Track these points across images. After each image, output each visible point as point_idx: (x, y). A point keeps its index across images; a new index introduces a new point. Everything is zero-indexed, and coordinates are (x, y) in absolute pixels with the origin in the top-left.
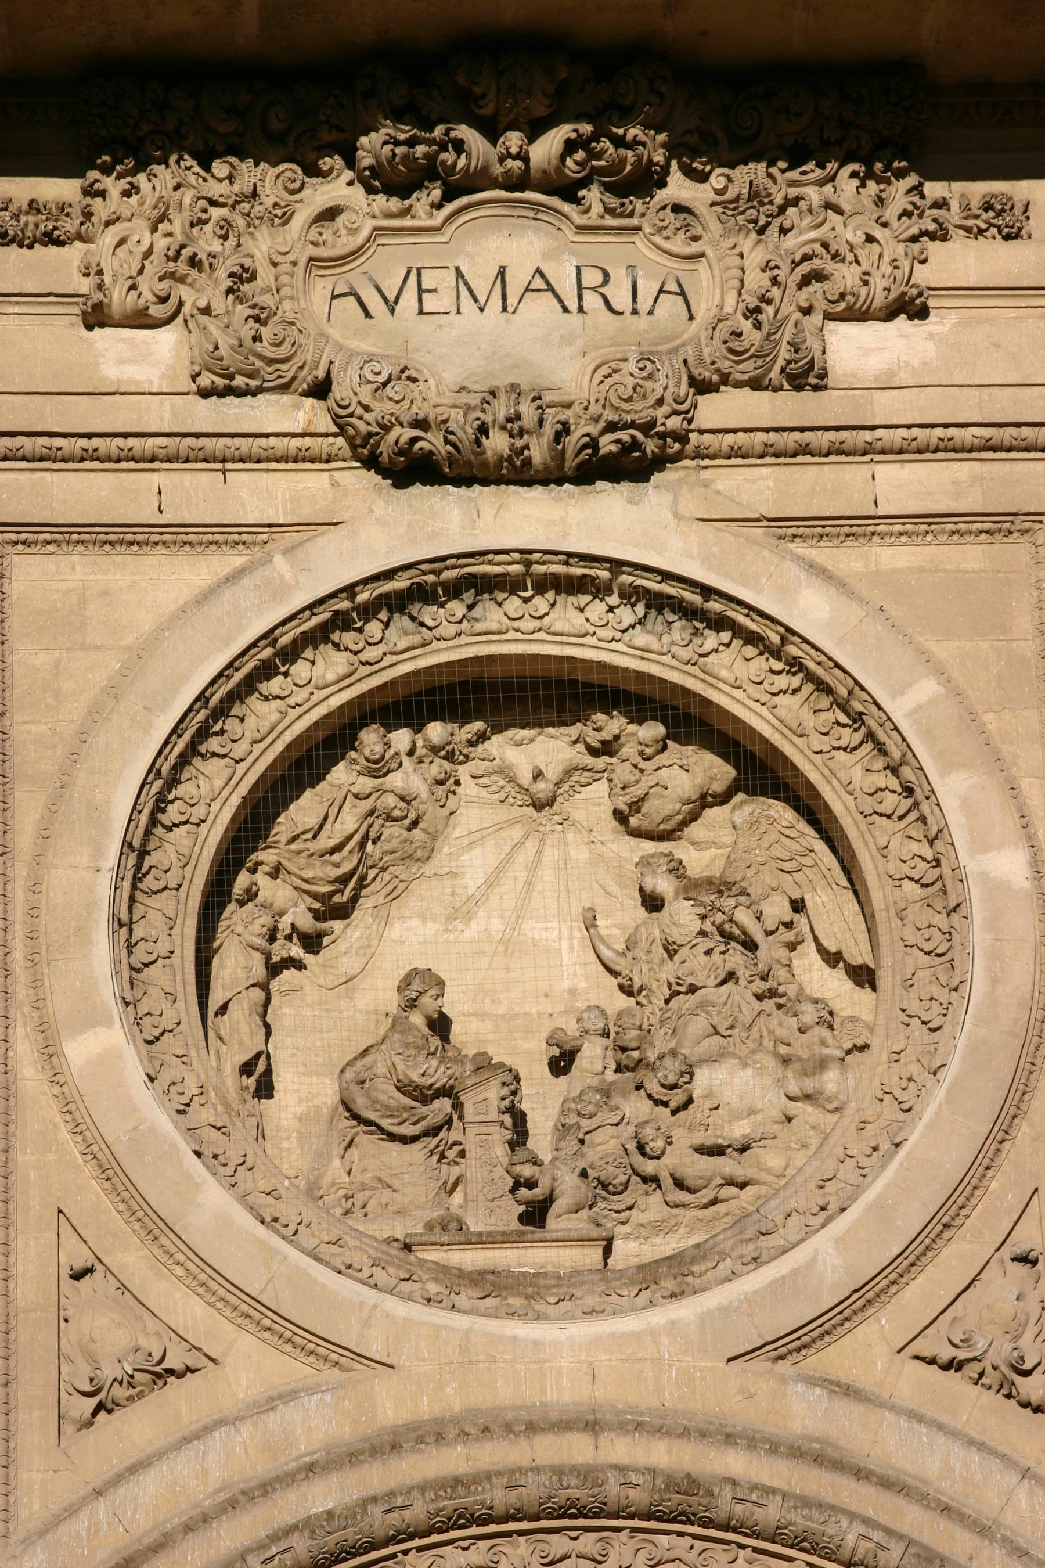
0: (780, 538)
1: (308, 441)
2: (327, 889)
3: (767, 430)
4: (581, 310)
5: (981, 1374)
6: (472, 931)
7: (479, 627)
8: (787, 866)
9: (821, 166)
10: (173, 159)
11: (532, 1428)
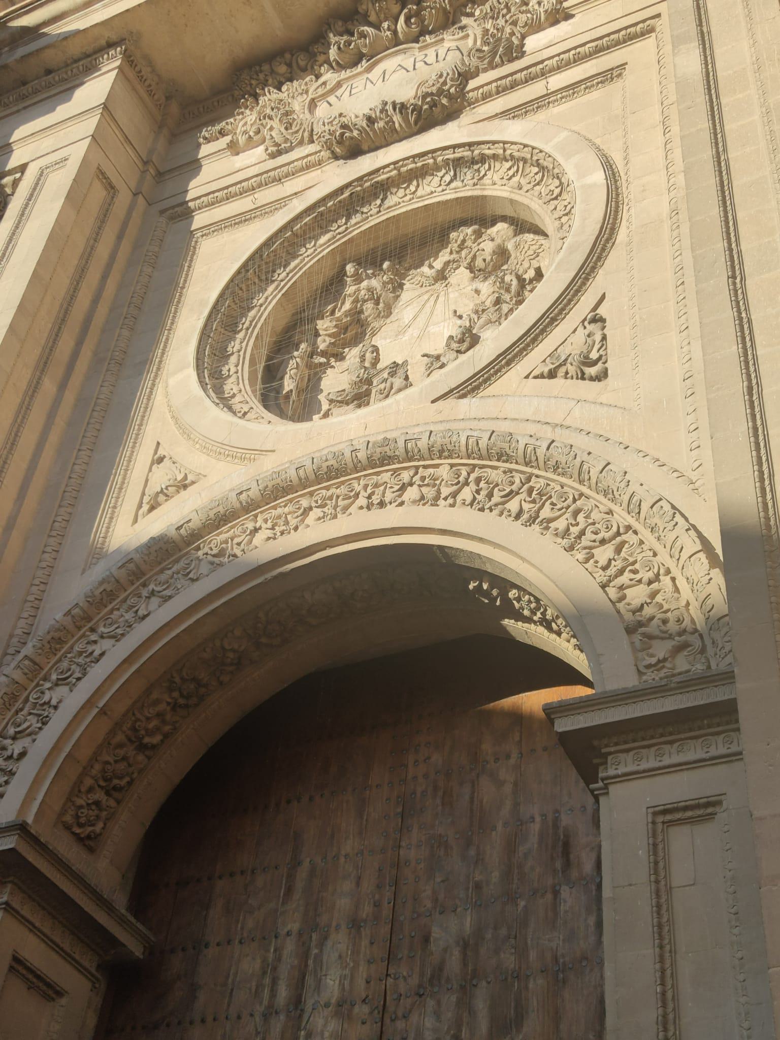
2: (334, 330)
5: (567, 373)
6: (406, 337)
8: (532, 257)
10: (266, 90)
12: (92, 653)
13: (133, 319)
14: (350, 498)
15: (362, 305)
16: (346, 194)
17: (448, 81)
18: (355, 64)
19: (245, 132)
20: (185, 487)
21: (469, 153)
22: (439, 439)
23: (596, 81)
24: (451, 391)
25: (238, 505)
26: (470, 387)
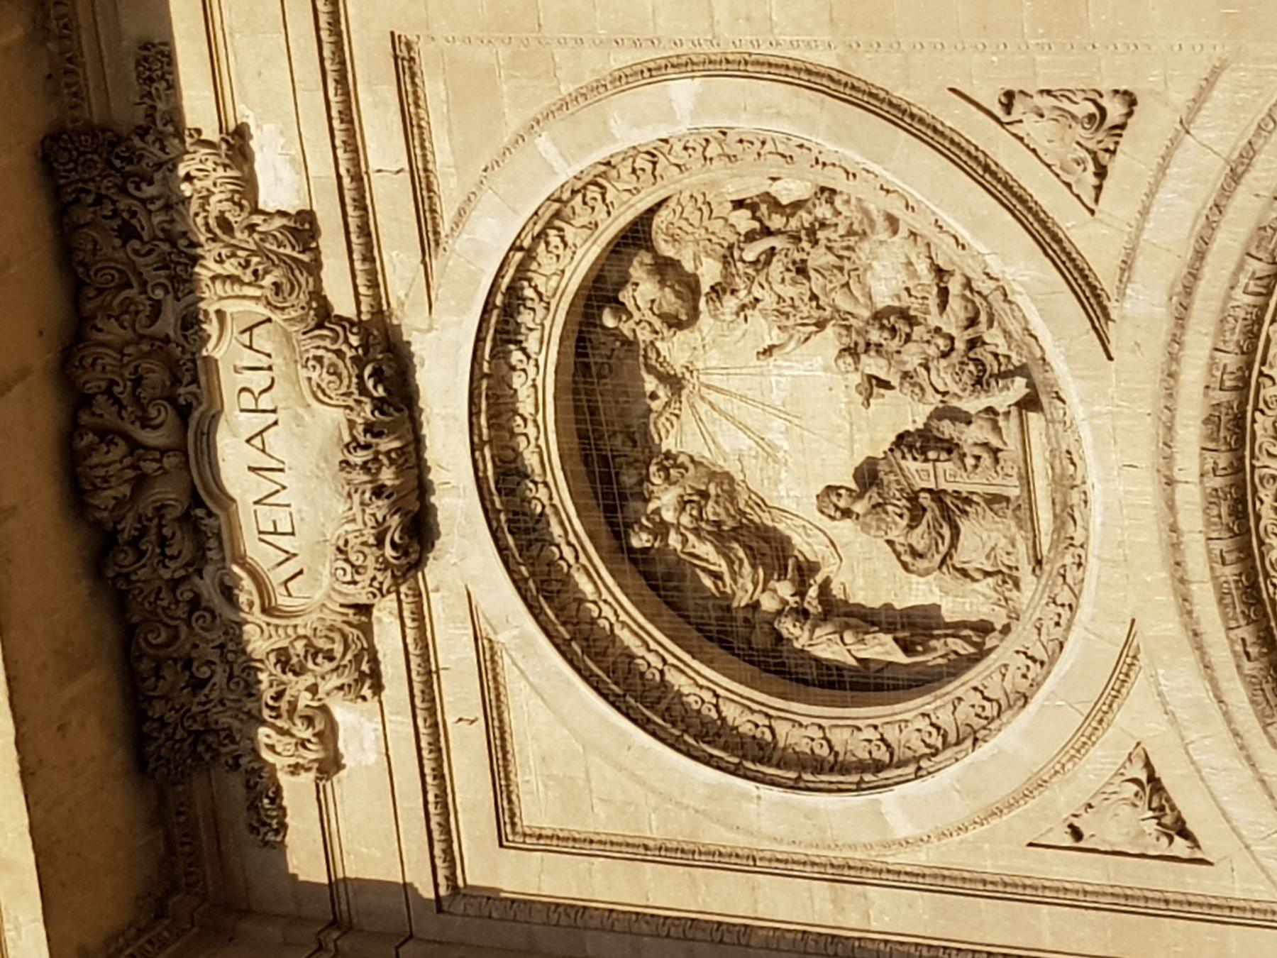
1: (406, 614)
3: (351, 261)
17: (335, 347)
21: (496, 312)
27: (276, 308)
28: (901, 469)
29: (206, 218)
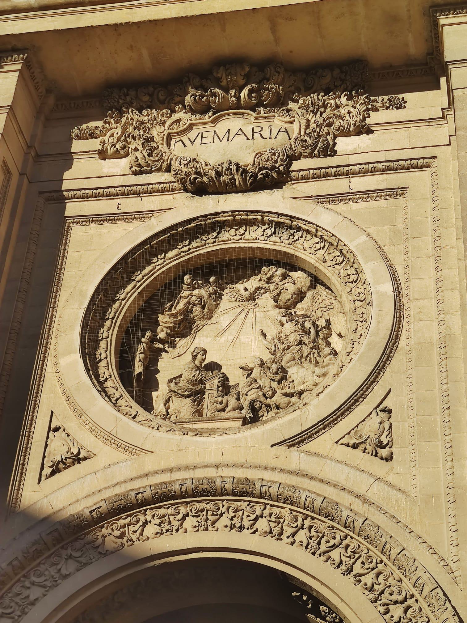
0: (318, 202)
2: (172, 325)
4: (253, 138)
5: (365, 449)
6: (223, 339)
7: (220, 239)
8: (324, 309)
9: (334, 94)
10: (130, 110)
11: (195, 467)
12: (28, 597)
13: (25, 293)
14: (217, 515)
15: (192, 307)
16: (193, 225)
17: (279, 160)
18: (203, 112)
19: (114, 145)
20: (79, 460)
21: (289, 222)
22: (286, 492)
23: (385, 193)
24: (285, 440)
25: (135, 502)
26: (297, 440)
27: (296, 140)
28: (215, 377)
29: (333, 118)
